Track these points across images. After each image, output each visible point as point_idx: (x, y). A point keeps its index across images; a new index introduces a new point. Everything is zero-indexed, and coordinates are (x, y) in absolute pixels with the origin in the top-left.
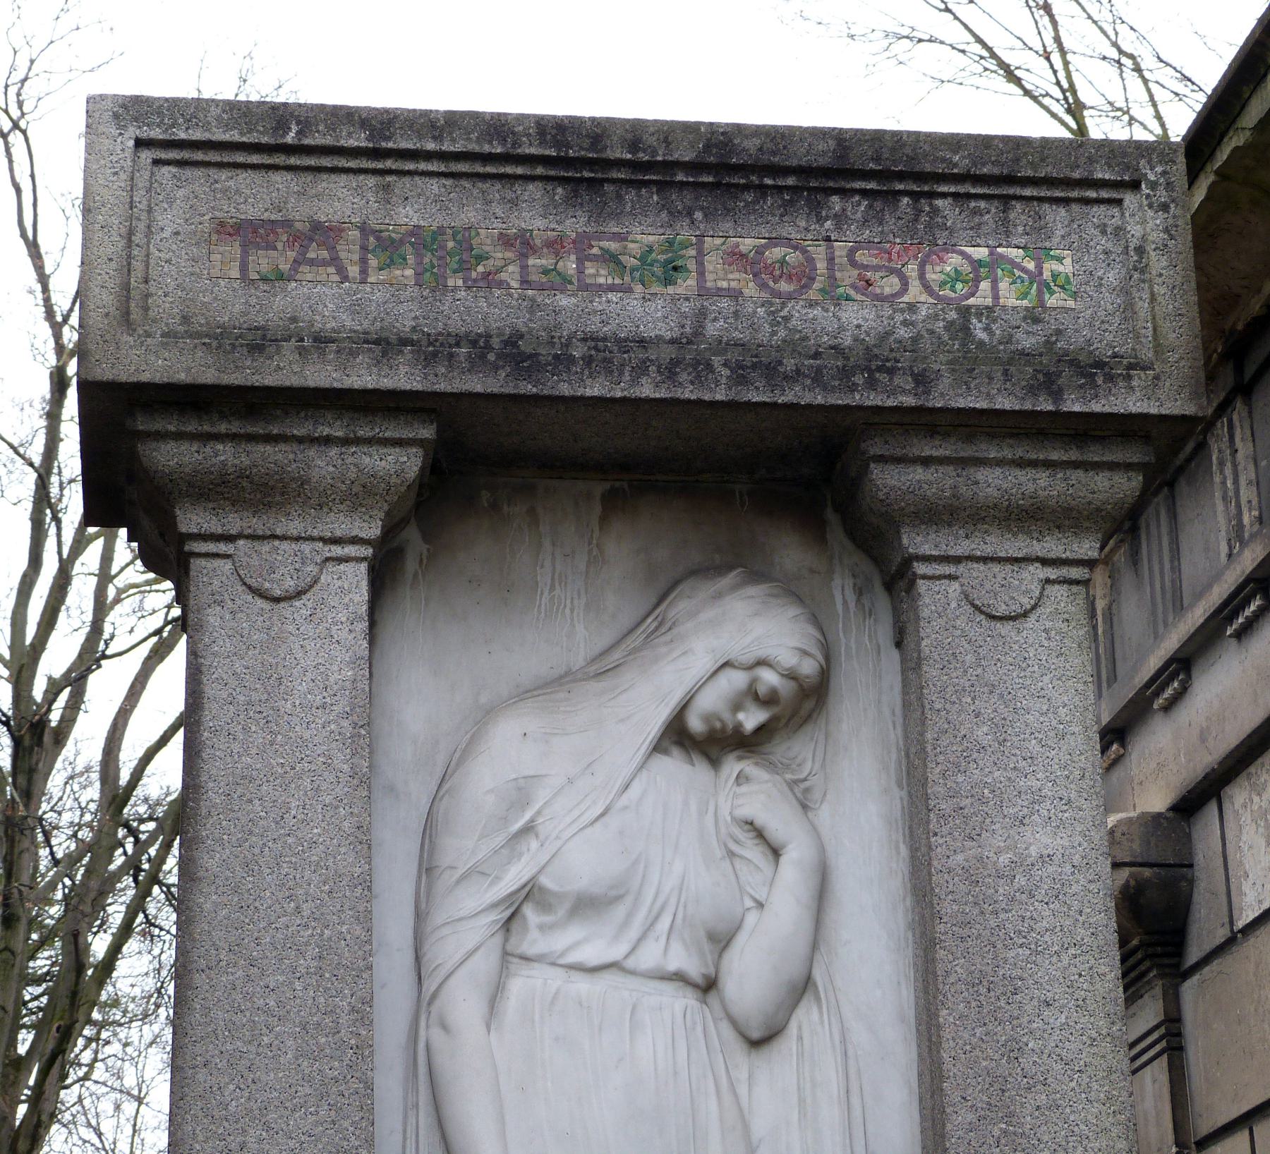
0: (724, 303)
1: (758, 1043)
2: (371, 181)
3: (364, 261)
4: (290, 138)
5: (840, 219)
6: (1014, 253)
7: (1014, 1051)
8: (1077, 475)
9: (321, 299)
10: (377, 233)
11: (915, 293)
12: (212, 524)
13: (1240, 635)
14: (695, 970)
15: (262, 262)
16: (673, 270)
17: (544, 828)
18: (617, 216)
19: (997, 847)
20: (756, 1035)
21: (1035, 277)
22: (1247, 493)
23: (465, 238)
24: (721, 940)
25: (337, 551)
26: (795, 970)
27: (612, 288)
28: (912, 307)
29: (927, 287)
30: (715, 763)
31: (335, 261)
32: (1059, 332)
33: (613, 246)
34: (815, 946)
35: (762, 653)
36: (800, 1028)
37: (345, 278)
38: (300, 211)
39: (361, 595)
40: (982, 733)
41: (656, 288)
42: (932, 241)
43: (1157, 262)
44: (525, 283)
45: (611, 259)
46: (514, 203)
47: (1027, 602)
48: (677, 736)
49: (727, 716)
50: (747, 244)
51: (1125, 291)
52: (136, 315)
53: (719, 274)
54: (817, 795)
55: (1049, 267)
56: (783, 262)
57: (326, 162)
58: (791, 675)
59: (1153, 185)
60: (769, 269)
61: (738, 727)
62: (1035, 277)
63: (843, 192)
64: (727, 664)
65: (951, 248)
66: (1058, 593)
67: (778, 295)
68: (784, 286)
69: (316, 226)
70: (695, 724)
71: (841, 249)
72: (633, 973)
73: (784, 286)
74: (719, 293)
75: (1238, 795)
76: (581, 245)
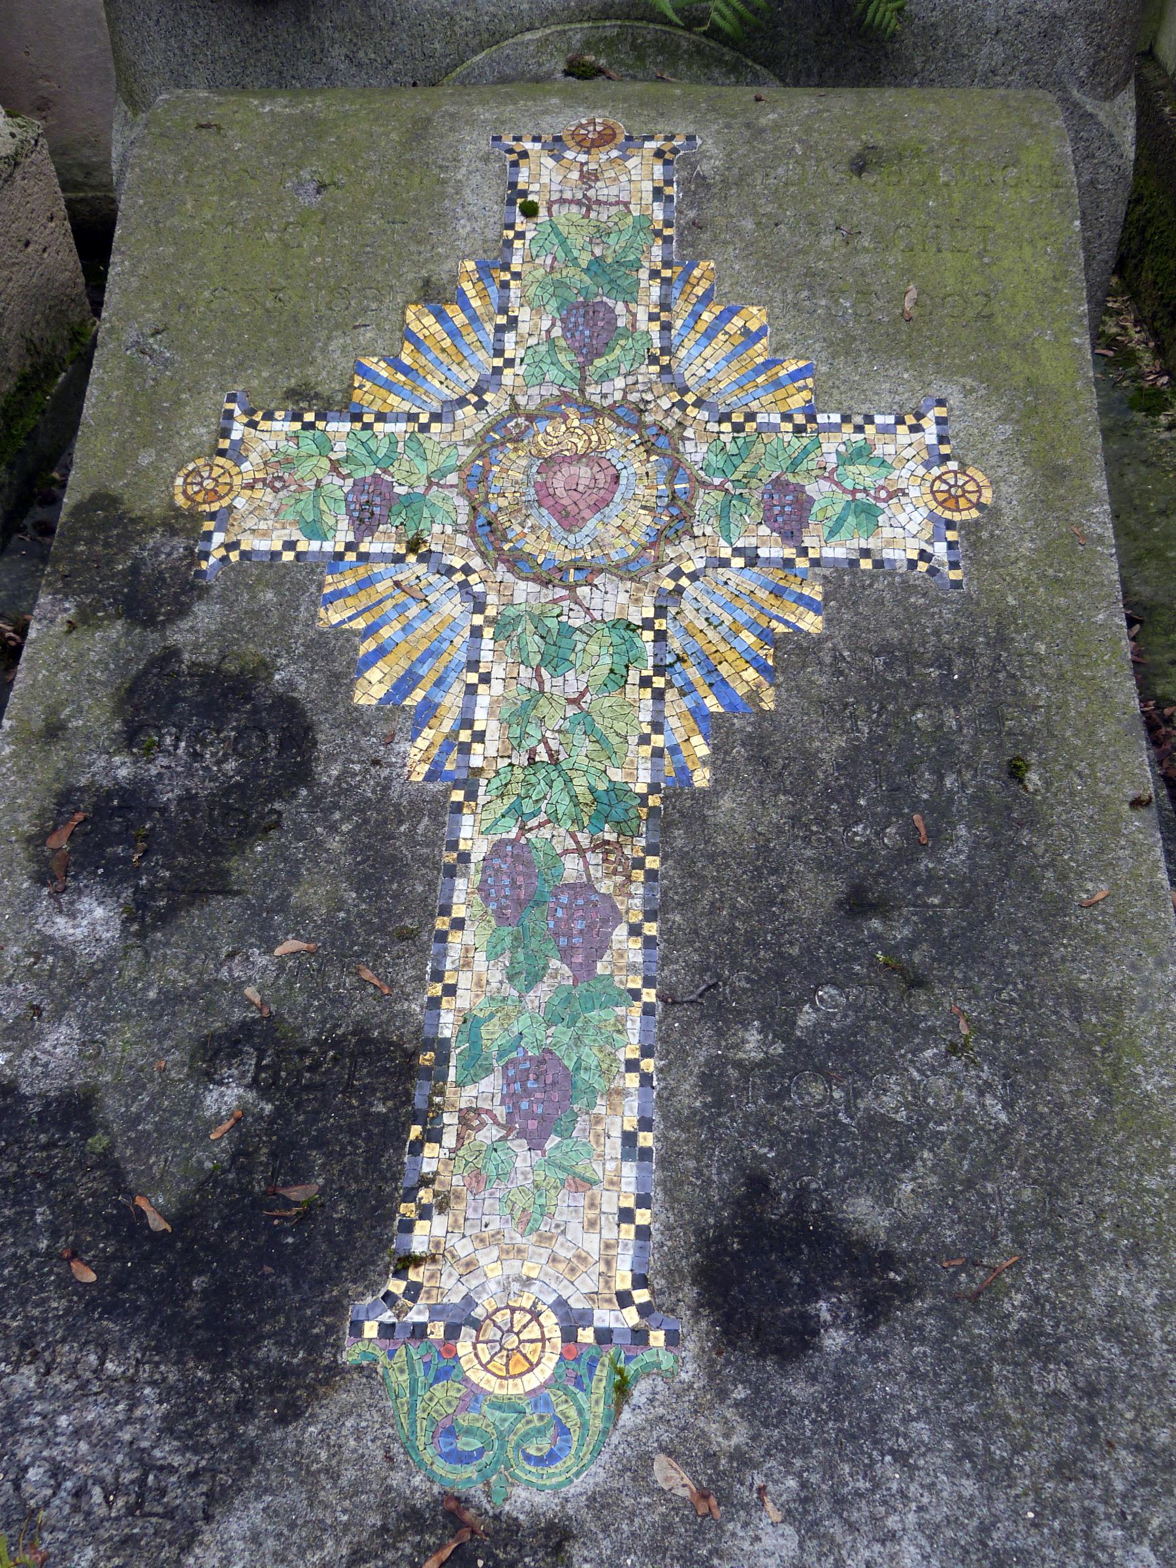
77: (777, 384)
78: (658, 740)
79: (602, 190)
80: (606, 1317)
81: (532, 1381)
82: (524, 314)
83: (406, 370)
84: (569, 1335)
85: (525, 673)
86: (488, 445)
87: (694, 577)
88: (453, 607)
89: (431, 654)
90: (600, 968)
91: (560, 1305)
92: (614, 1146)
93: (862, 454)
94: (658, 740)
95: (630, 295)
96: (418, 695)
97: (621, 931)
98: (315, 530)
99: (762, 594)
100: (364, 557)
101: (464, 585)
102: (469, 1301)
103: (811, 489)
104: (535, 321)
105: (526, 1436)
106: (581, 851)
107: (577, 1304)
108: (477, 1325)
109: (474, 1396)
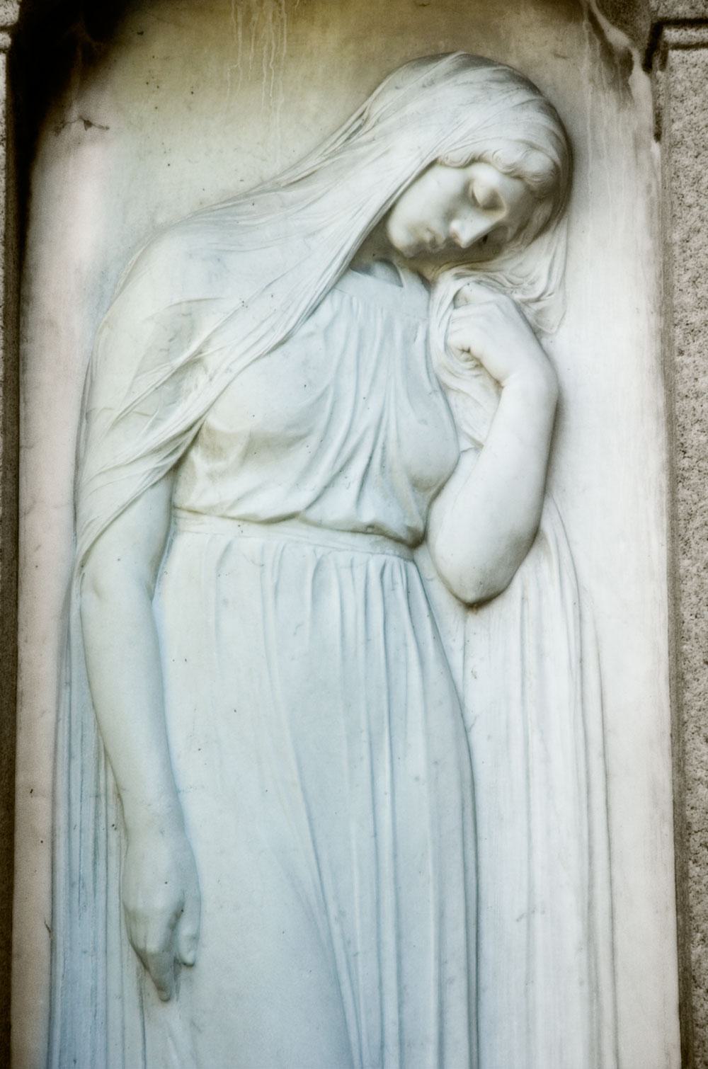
1: (476, 606)
14: (396, 521)
17: (212, 359)
20: (471, 596)
24: (431, 488)
26: (518, 520)
30: (428, 284)
34: (545, 489)
35: (477, 149)
36: (524, 588)
49: (436, 225)
54: (552, 318)
58: (514, 174)
61: (451, 242)
64: (432, 165)
70: (399, 234)
72: (318, 525)
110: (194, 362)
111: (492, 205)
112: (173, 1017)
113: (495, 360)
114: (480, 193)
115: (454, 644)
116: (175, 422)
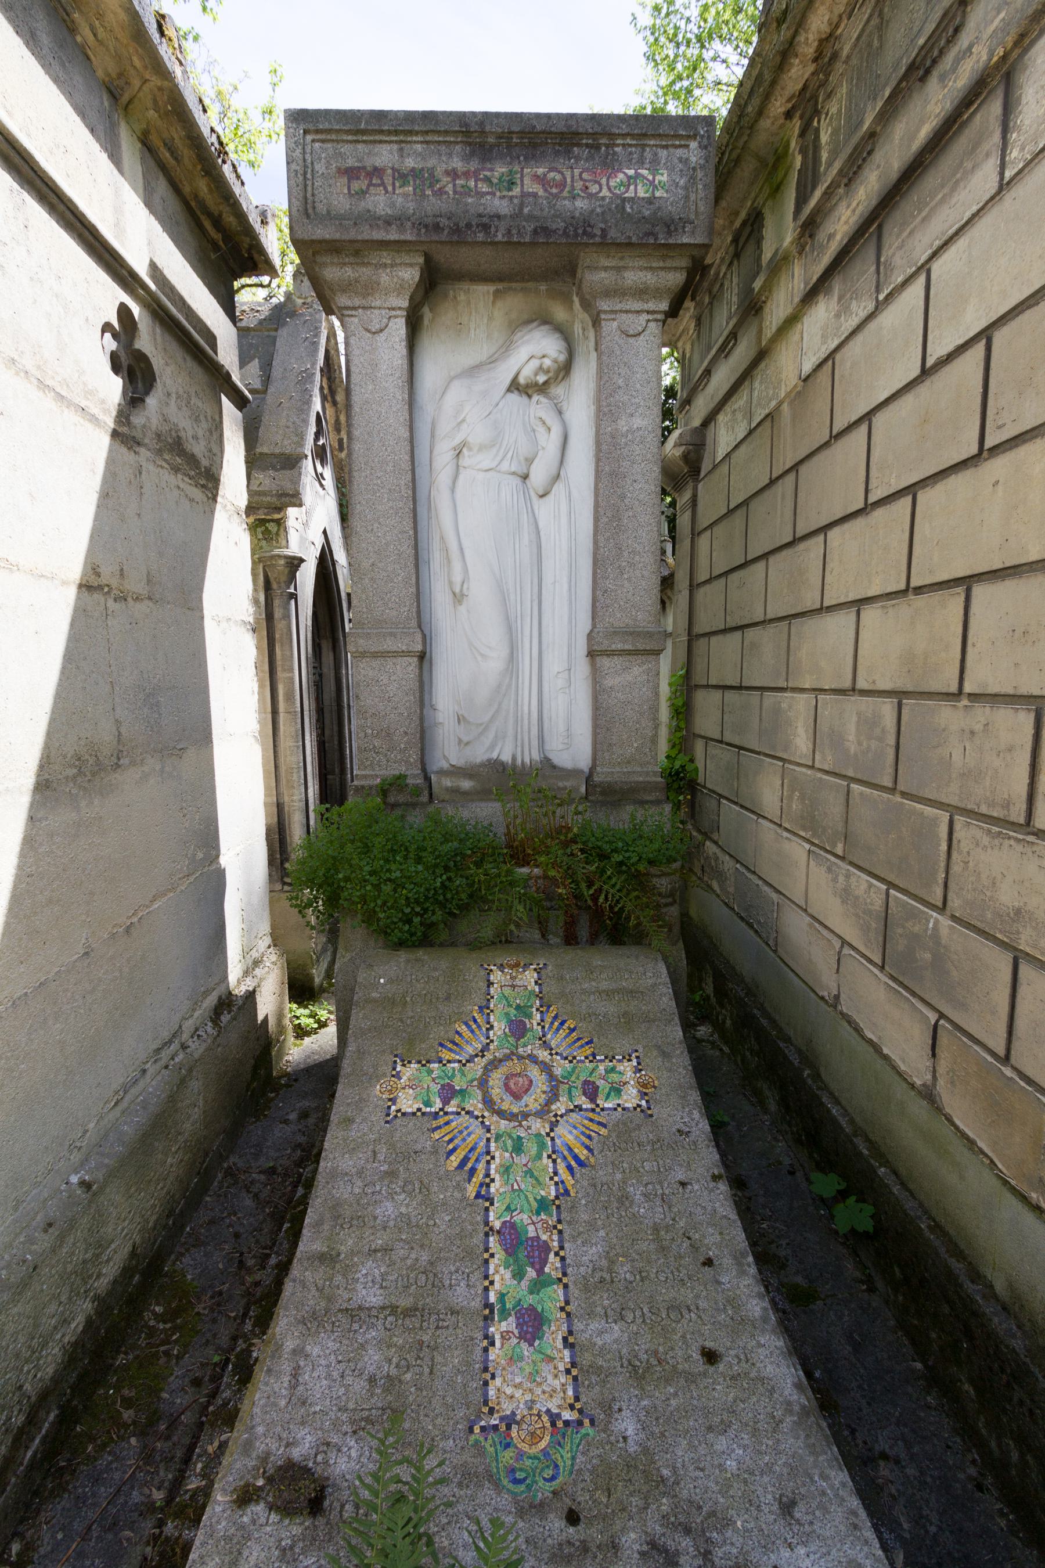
0: (531, 199)
1: (542, 496)
2: (395, 147)
3: (394, 184)
4: (363, 126)
5: (578, 159)
6: (645, 172)
7: (623, 497)
8: (662, 274)
9: (379, 202)
10: (398, 171)
11: (605, 192)
12: (349, 303)
13: (726, 357)
15: (356, 185)
16: (512, 183)
18: (490, 160)
19: (623, 425)
21: (652, 183)
22: (735, 299)
23: (432, 171)
24: (530, 461)
25: (394, 313)
26: (554, 472)
27: (488, 193)
28: (603, 198)
29: (609, 189)
30: (530, 397)
31: (383, 184)
32: (659, 208)
33: (488, 174)
37: (387, 192)
38: (369, 162)
39: (403, 331)
40: (620, 382)
41: (505, 193)
42: (611, 165)
43: (700, 174)
44: (455, 192)
45: (488, 180)
46: (450, 155)
47: (640, 329)
48: (514, 386)
50: (540, 171)
51: (686, 188)
52: (310, 211)
53: (531, 187)
55: (658, 178)
56: (554, 179)
57: (377, 138)
58: (555, 361)
59: (702, 137)
60: (549, 182)
62: (652, 183)
63: (578, 145)
65: (620, 170)
66: (652, 325)
67: (551, 194)
68: (554, 191)
69: (376, 169)
70: (522, 380)
71: (577, 172)
73: (554, 191)
74: (529, 194)
75: (721, 418)
76: (476, 173)
77: (582, 1046)
78: (556, 1179)
79: (517, 982)
80: (567, 1415)
81: (543, 1444)
82: (495, 1024)
83: (457, 1045)
84: (553, 1424)
85: (507, 1155)
86: (488, 1069)
87: (562, 1116)
88: (480, 1131)
89: (472, 1150)
90: (547, 1270)
91: (548, 1411)
92: (559, 1344)
93: (613, 1070)
94: (556, 1179)
95: (530, 1016)
96: (469, 1165)
97: (552, 1255)
98: (428, 1104)
99: (586, 1122)
100: (446, 1113)
101: (482, 1123)
102: (513, 1413)
103: (598, 1083)
104: (500, 1026)
105: (542, 1470)
106: (534, 1223)
107: (555, 1411)
108: (518, 1423)
109: (520, 1455)
110: (463, 420)
111: (548, 371)
112: (462, 609)
113: (549, 422)
114: (545, 367)
115: (536, 507)
116: (457, 440)
